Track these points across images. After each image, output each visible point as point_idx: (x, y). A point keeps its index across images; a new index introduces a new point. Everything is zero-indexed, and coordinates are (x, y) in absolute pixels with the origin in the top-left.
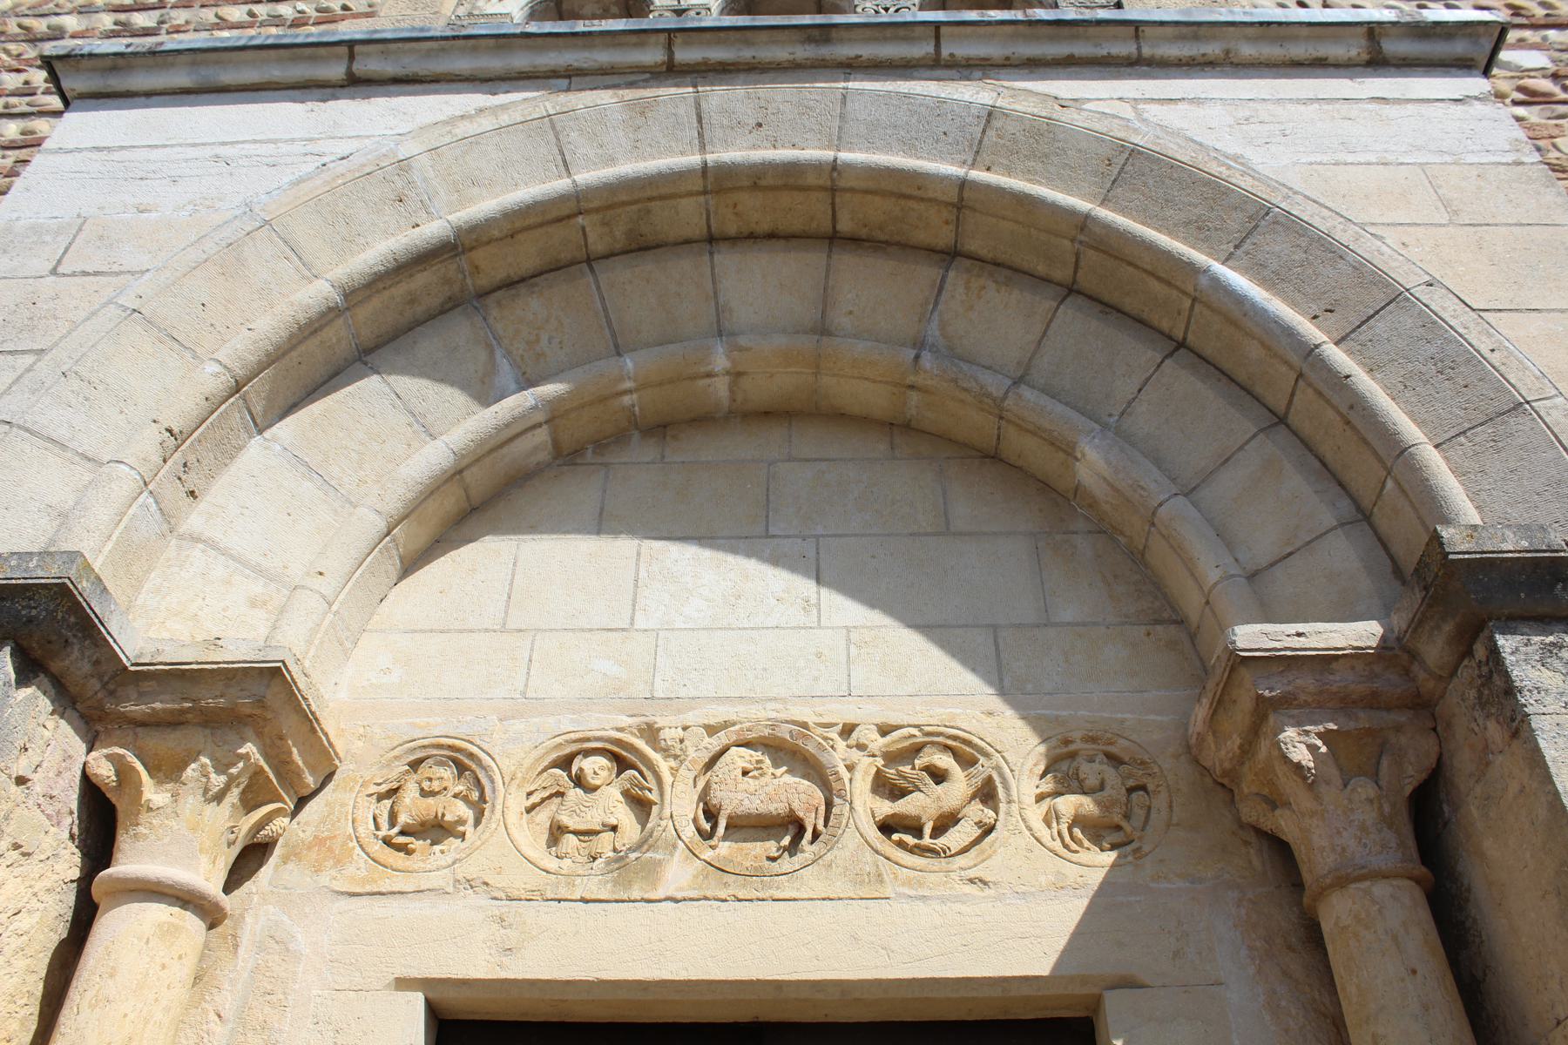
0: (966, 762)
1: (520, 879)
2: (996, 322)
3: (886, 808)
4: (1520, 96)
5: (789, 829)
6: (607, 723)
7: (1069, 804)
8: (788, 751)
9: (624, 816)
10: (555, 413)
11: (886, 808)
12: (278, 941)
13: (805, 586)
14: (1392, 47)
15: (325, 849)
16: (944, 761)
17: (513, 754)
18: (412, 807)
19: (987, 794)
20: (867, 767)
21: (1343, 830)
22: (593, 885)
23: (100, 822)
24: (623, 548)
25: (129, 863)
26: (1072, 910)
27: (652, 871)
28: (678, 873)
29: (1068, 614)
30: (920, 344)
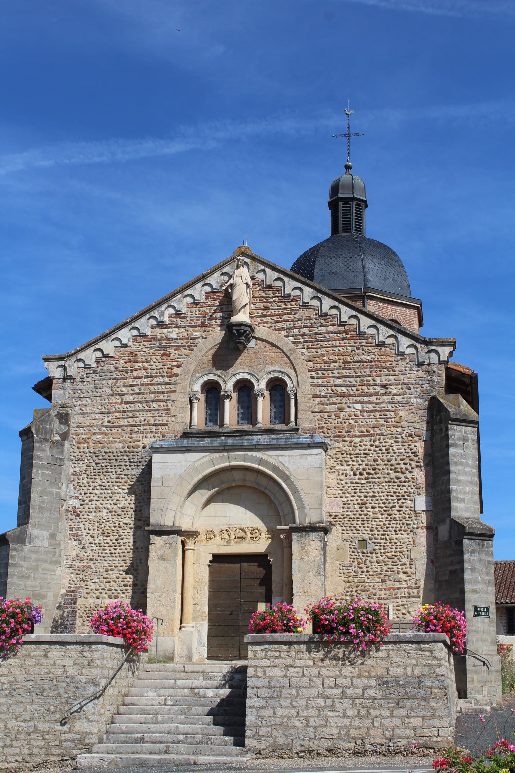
0: (259, 531)
1: (219, 544)
2: (264, 481)
3: (251, 536)
4: (353, 417)
5: (242, 538)
6: (226, 527)
7: (267, 536)
8: (242, 530)
9: (227, 537)
10: (216, 491)
11: (251, 536)
12: (198, 550)
13: (244, 509)
14: (311, 445)
15: (201, 541)
16: (257, 531)
17: (217, 531)
18: (208, 536)
19: (260, 534)
20: (250, 531)
21: (285, 543)
22: (225, 544)
23: (183, 543)
24: (226, 505)
25: (186, 548)
26: (266, 546)
27: (230, 543)
28: (232, 543)
29: (270, 514)
30: (255, 482)
